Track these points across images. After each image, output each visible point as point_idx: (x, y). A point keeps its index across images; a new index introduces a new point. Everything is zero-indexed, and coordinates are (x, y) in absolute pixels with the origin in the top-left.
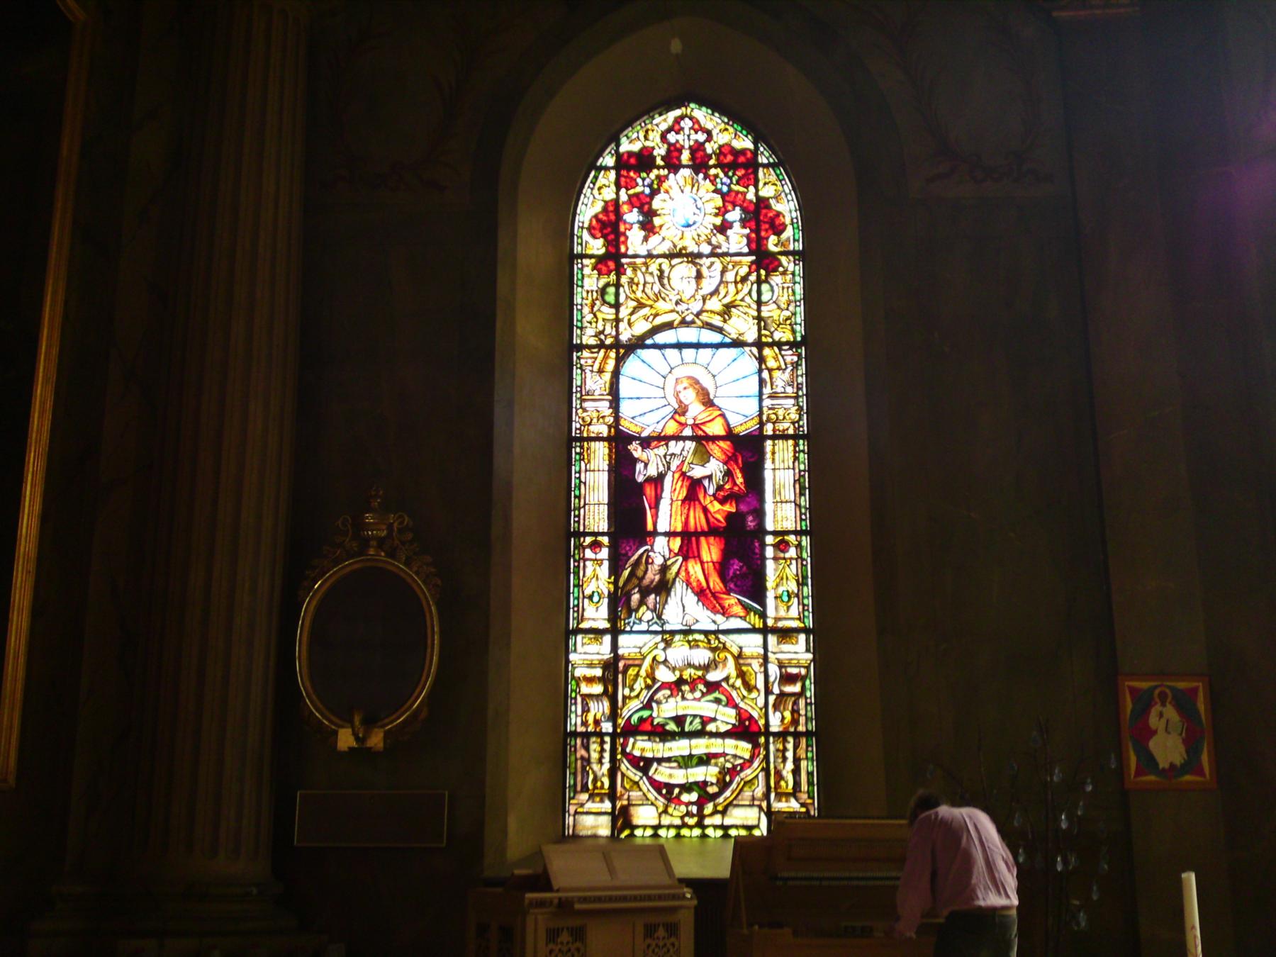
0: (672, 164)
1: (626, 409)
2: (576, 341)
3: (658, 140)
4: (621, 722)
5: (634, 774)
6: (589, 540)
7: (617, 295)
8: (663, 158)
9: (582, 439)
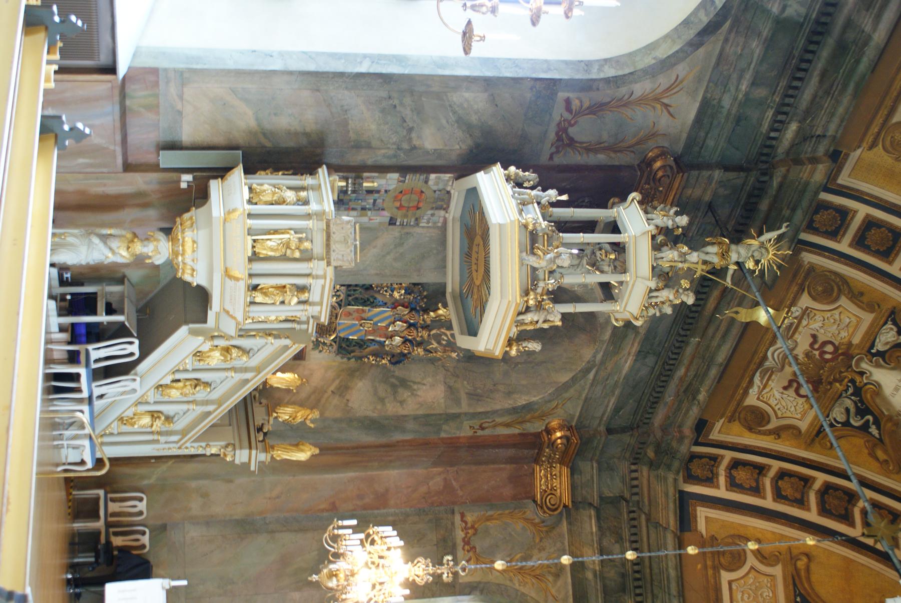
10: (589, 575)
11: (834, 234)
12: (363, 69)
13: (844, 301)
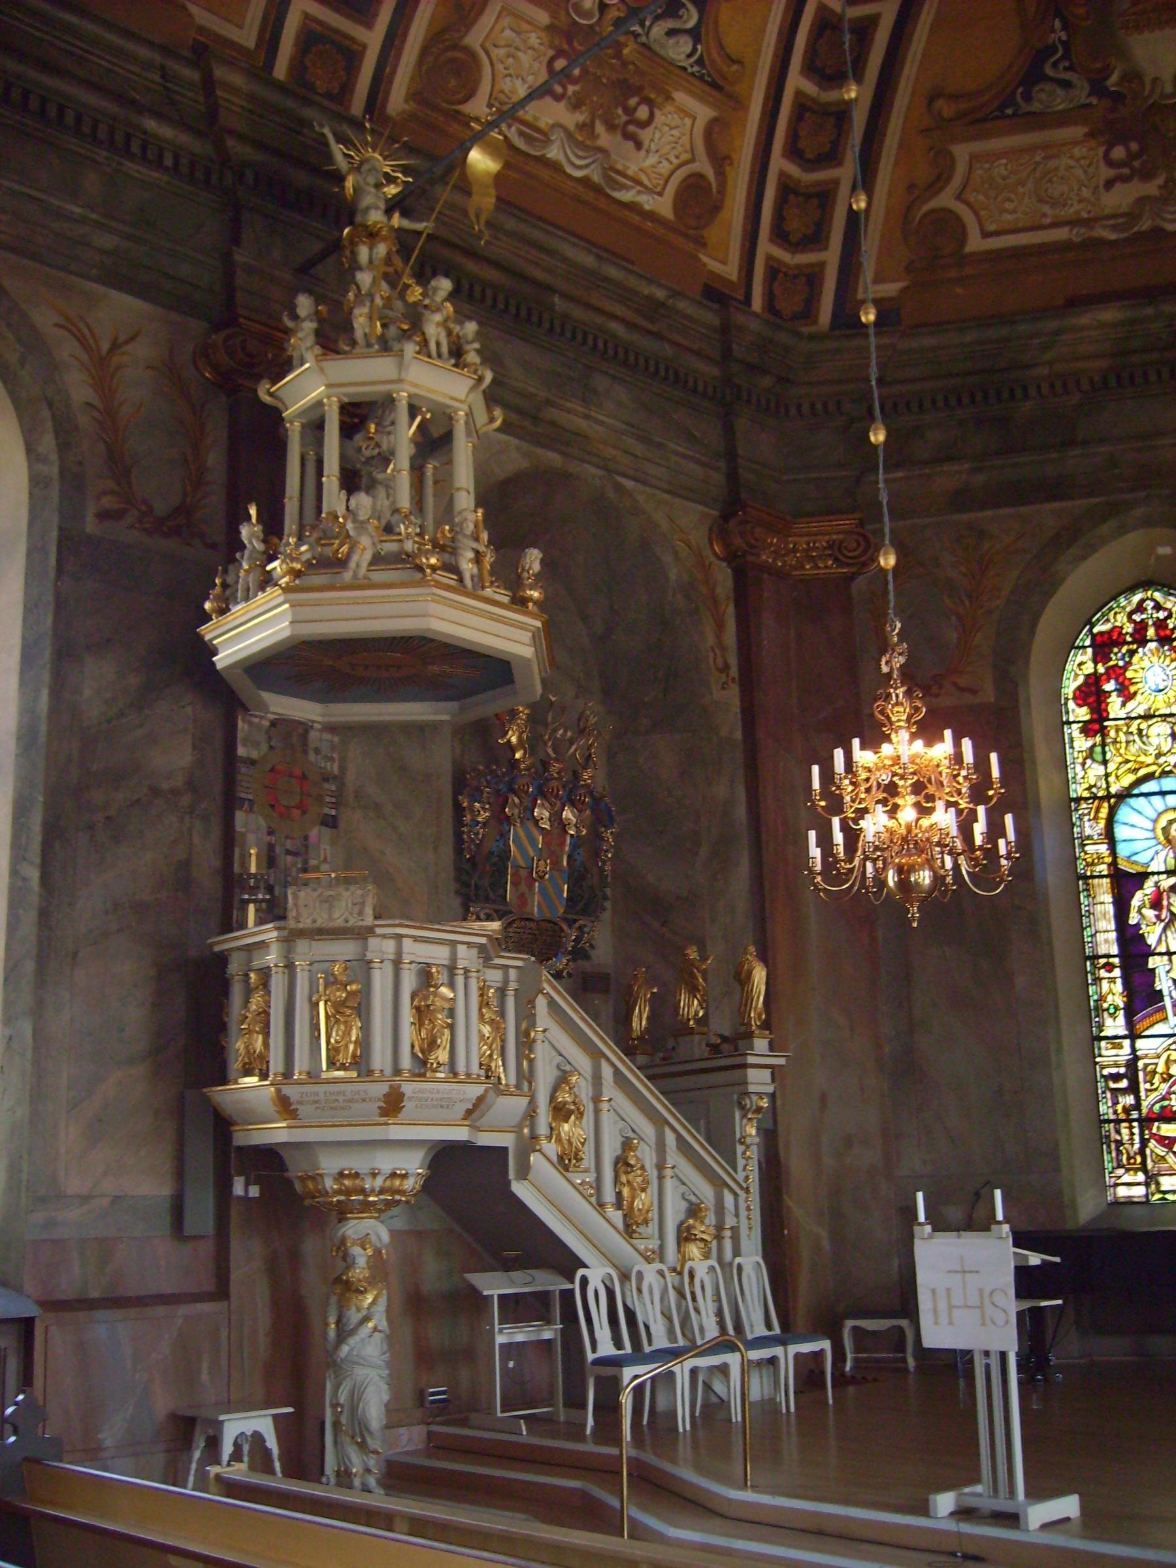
0: (1142, 641)
1: (1123, 850)
2: (1073, 795)
3: (1125, 620)
4: (1145, 1111)
5: (1161, 1151)
6: (1103, 961)
7: (1104, 753)
8: (1131, 635)
9: (1085, 878)
10: (980, 479)
11: (351, 55)
12: (34, 875)
13: (474, 39)
